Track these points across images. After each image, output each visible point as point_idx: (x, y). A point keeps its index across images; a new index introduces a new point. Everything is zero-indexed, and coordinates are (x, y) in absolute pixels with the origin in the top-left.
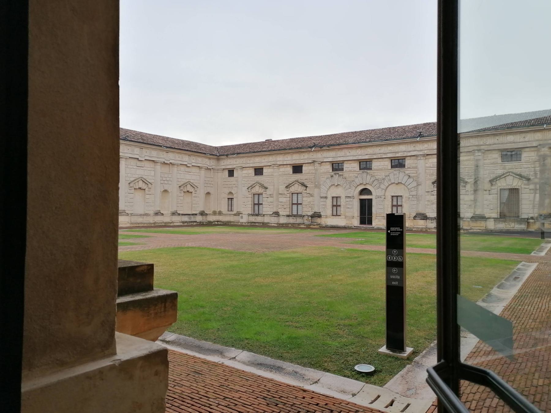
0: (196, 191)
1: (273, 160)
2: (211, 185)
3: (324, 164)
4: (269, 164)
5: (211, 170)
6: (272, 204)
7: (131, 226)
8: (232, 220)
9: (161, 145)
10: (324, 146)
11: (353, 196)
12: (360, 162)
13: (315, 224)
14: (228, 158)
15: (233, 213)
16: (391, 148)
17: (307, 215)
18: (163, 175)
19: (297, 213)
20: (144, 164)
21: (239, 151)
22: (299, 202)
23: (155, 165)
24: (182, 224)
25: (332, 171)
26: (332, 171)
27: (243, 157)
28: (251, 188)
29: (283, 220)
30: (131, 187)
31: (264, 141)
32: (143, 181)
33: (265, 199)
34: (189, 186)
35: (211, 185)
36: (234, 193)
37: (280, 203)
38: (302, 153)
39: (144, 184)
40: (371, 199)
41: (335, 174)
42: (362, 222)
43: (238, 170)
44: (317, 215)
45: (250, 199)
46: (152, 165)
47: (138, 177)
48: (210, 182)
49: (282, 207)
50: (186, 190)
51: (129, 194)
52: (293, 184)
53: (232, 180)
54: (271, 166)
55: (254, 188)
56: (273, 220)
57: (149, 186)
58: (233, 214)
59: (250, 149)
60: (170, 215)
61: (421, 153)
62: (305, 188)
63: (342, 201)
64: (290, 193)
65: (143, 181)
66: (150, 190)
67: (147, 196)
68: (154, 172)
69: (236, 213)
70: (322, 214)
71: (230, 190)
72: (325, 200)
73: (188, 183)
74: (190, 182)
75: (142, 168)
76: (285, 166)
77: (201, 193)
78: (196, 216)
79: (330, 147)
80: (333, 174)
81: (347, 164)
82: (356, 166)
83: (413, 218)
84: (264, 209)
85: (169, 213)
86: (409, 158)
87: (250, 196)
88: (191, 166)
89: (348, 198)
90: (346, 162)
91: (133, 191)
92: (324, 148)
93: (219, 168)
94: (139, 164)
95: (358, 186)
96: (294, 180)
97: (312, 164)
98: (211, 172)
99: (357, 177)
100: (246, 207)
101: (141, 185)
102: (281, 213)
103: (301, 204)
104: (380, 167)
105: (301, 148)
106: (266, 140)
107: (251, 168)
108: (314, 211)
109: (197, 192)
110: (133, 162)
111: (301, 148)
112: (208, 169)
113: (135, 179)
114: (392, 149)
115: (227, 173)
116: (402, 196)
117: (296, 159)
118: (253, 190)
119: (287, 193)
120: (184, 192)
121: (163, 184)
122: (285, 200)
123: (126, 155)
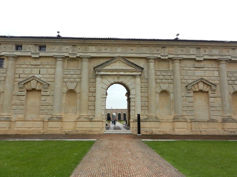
18: (230, 75)
20: (203, 64)
23: (218, 64)
30: (190, 90)
32: (204, 83)
46: (214, 65)
47: (197, 79)
51: (187, 98)
57: (212, 87)
65: (204, 83)
67: (211, 100)
68: (218, 72)
75: (201, 69)
91: (192, 94)
94: (197, 65)
101: (201, 86)
110: (189, 64)
113: (194, 80)
121: (232, 84)
123: (180, 56)
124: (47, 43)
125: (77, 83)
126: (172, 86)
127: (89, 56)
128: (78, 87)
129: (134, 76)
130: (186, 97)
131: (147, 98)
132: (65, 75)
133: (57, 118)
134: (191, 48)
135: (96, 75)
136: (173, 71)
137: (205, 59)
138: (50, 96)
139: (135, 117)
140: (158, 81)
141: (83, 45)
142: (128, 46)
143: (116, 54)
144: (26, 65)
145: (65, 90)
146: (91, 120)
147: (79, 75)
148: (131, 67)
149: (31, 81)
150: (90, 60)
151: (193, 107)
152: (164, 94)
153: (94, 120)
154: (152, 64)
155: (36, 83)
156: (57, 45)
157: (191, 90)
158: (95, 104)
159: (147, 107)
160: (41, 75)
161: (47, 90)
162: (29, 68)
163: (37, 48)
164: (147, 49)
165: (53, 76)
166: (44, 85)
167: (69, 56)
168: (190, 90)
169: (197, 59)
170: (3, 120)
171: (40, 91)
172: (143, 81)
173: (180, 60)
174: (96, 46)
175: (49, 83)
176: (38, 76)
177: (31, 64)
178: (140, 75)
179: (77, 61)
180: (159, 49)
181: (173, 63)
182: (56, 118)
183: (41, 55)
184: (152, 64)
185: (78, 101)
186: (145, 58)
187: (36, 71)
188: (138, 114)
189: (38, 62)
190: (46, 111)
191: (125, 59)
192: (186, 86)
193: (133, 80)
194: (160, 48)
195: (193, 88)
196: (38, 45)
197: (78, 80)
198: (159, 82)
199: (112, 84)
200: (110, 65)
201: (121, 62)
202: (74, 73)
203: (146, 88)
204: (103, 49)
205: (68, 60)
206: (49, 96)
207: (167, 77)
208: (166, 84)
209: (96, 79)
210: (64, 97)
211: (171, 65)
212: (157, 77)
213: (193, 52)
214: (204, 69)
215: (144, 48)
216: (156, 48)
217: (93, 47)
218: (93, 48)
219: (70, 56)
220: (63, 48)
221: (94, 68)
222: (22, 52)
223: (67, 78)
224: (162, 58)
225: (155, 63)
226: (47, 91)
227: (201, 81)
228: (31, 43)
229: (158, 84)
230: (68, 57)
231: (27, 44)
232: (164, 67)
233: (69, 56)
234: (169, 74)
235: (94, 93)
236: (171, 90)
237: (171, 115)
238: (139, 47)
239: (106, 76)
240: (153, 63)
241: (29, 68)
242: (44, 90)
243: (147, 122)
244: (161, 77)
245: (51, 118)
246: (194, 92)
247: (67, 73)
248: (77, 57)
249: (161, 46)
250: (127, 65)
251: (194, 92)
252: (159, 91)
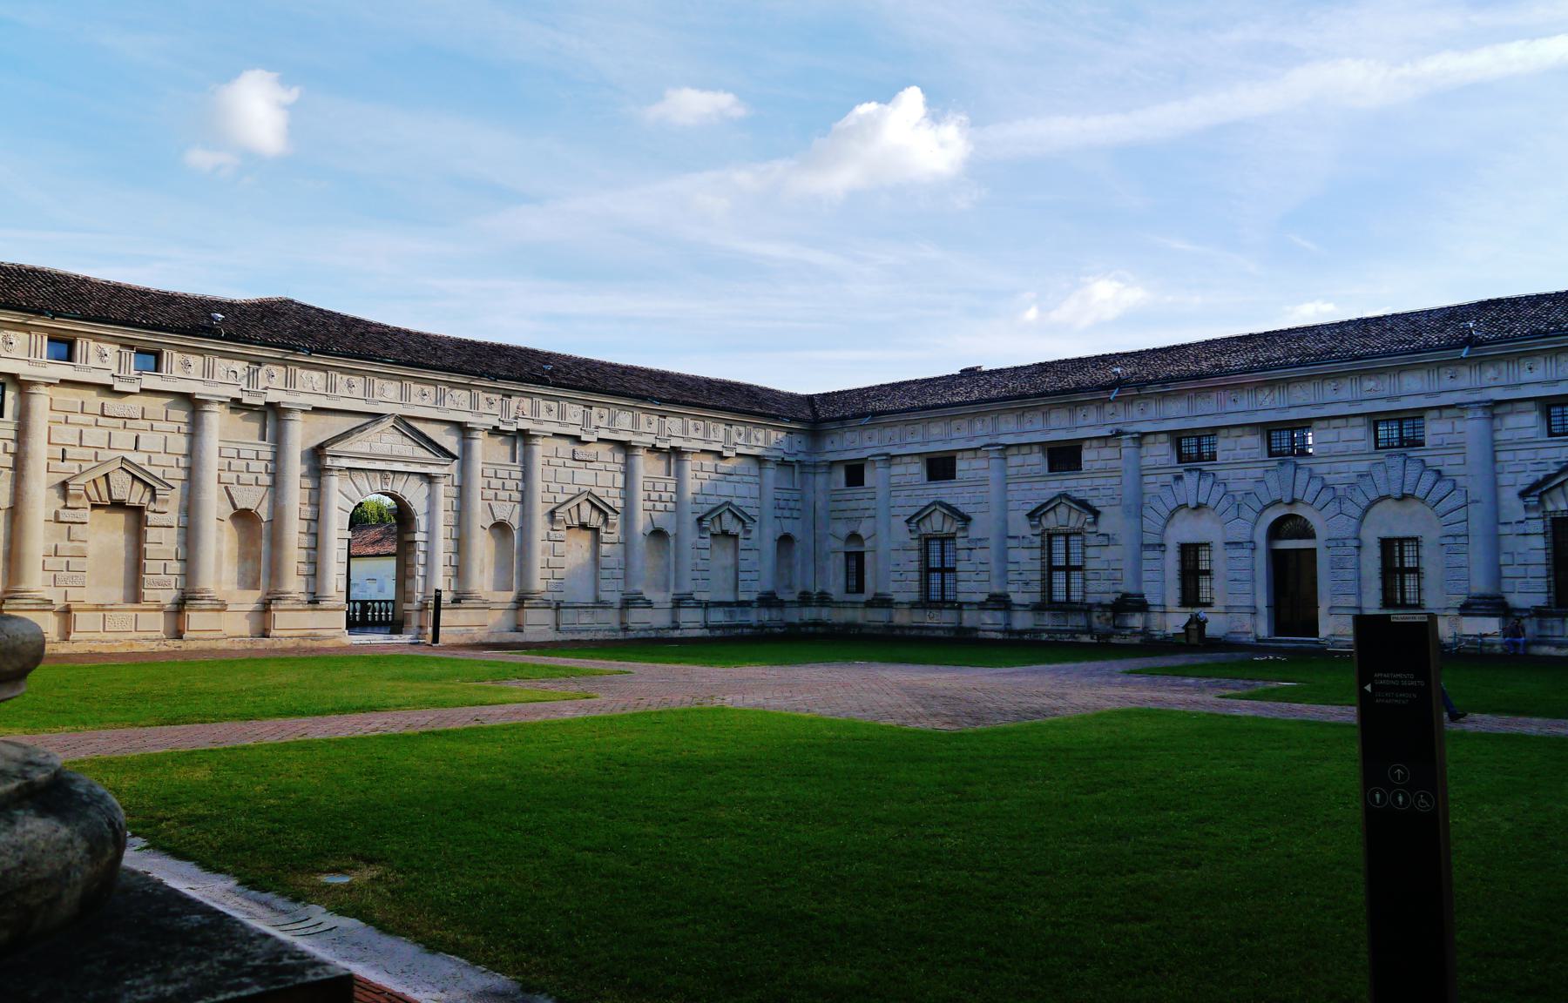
0: (749, 531)
1: (984, 432)
2: (795, 514)
3: (1151, 439)
4: (974, 444)
5: (794, 466)
6: (982, 567)
7: (557, 638)
8: (860, 620)
9: (645, 393)
10: (1150, 382)
11: (1250, 542)
12: (1268, 430)
13: (1128, 632)
14: (846, 429)
15: (864, 598)
16: (1372, 384)
17: (1100, 605)
19: (1068, 596)
21: (878, 406)
22: (947, 566)
24: (706, 632)
25: (1179, 463)
26: (1179, 463)
27: (891, 425)
28: (919, 521)
29: (1022, 621)
31: (957, 372)
32: (593, 505)
33: (963, 554)
34: (727, 517)
35: (795, 514)
36: (864, 537)
37: (1011, 567)
38: (1078, 408)
39: (595, 514)
40: (1314, 550)
41: (1189, 470)
42: (1280, 624)
43: (877, 466)
44: (1132, 603)
45: (915, 555)
48: (792, 504)
49: (1018, 577)
50: (717, 530)
52: (1053, 505)
53: (859, 496)
54: (979, 449)
55: (927, 521)
56: (989, 621)
58: (864, 600)
59: (914, 398)
60: (670, 605)
61: (1477, 397)
62: (1090, 518)
63: (1217, 561)
64: (1043, 533)
66: (612, 531)
69: (873, 599)
70: (1149, 599)
71: (852, 527)
72: (1156, 554)
73: (727, 507)
74: (730, 503)
76: (1025, 450)
77: (764, 537)
78: (749, 608)
79: (1168, 387)
80: (1181, 470)
81: (1227, 437)
82: (1253, 444)
83: (1456, 613)
84: (961, 587)
85: (670, 597)
86: (1435, 413)
87: (915, 544)
88: (734, 455)
89: (1234, 546)
90: (1223, 432)
92: (1150, 389)
93: (818, 458)
95: (1266, 507)
96: (1056, 492)
97: (1112, 443)
98: (794, 473)
99: (1260, 481)
100: (903, 578)
102: (1016, 598)
103: (1078, 568)
104: (1340, 447)
105: (1076, 390)
106: (961, 371)
107: (916, 459)
108: (1123, 588)
109: (755, 534)
111: (1076, 390)
112: (783, 464)
113: (571, 496)
114: (1377, 386)
115: (840, 475)
116: (1415, 539)
117: (1059, 427)
118: (924, 525)
119: (1033, 535)
120: (712, 535)
122: (1027, 560)
161: (165, 510)
170: (34, 607)
187: (123, 439)
188: (437, 591)
191: (405, 424)
214: (595, 465)
237: (512, 590)
243: (459, 611)
249: (502, 391)
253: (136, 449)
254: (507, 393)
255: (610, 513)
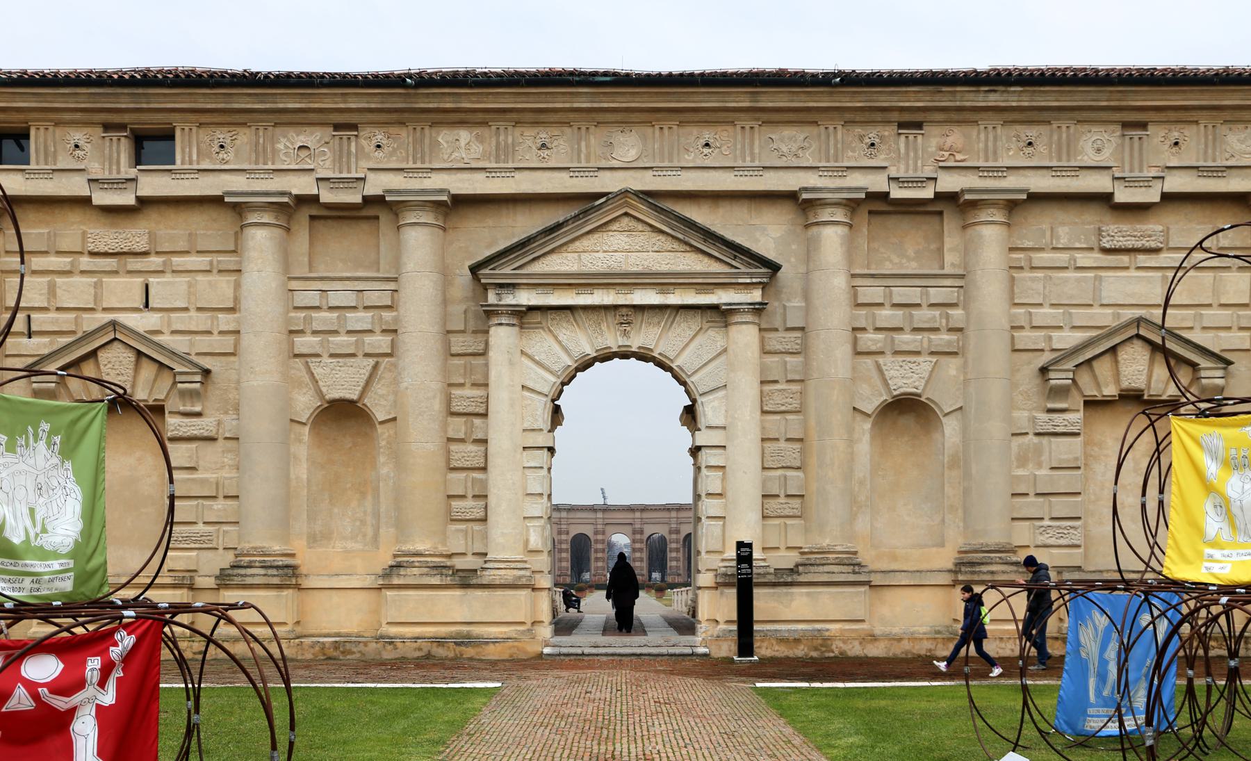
20: (1160, 228)
30: (1059, 392)
51: (1045, 440)
57: (1203, 374)
75: (1142, 259)
94: (1120, 232)
113: (1094, 333)
123: (1013, 181)
124: (177, 116)
125: (371, 361)
126: (951, 367)
127: (441, 191)
128: (379, 388)
129: (721, 315)
130: (1036, 440)
131: (797, 446)
132: (302, 314)
133: (270, 572)
134: (1086, 127)
135: (490, 313)
136: (962, 277)
137: (1167, 198)
138: (221, 442)
139: (723, 560)
140: (871, 340)
141: (402, 123)
142: (682, 124)
143: (608, 174)
144: (60, 253)
145: (305, 404)
146: (466, 580)
147: (387, 315)
148: (701, 257)
149: (100, 354)
150: (446, 216)
151: (1079, 499)
152: (907, 421)
153: (487, 577)
154: (832, 238)
155: (132, 366)
156: (244, 124)
157: (1074, 392)
158: (484, 484)
159: (796, 503)
160: (157, 315)
161: (198, 409)
162: (83, 272)
163: (123, 149)
164: (802, 137)
165: (225, 321)
166: (178, 378)
167: (315, 192)
168: (1059, 392)
169: (1122, 196)
171: (159, 410)
172: (777, 341)
173: (1012, 206)
174: (485, 124)
175: (206, 363)
176: (139, 322)
177: (91, 247)
178: (758, 309)
179: (365, 226)
180: (881, 138)
181: (965, 227)
182: (262, 571)
183: (144, 192)
184: (832, 238)
185: (385, 469)
186: (790, 197)
189: (134, 235)
190: (201, 527)
192: (1044, 370)
193: (712, 339)
194: (889, 131)
195: (1084, 379)
196: (121, 127)
197: (380, 342)
198: (873, 348)
199: (585, 365)
200: (572, 247)
201: (640, 227)
202: (350, 300)
203: (795, 387)
204: (527, 141)
205: (312, 218)
206: (212, 439)
207: (924, 316)
208: (920, 359)
209: (487, 332)
210: (303, 444)
211: (952, 239)
212: (862, 315)
213: (1099, 150)
215: (788, 132)
216: (858, 130)
217: (464, 135)
218: (463, 143)
219: (327, 197)
220: (281, 146)
221: (474, 269)
222: (34, 172)
223: (315, 333)
224: (896, 193)
225: (851, 226)
226: (199, 415)
227: (1138, 336)
228: (83, 119)
229: (869, 361)
230: (314, 199)
231: (57, 124)
232: (911, 252)
233: (318, 196)
234: (936, 295)
235: (477, 421)
236: (943, 397)
237: (942, 545)
238: (755, 124)
239: (551, 315)
240: (841, 230)
241: (83, 272)
242: (182, 408)
244: (887, 316)
245: (233, 567)
246: (1086, 402)
247: (312, 299)
248: (368, 201)
249: (896, 116)
250: (676, 245)
251: (1090, 404)
252: (872, 401)
253: (147, 305)
254: (907, 117)
255: (1203, 363)
